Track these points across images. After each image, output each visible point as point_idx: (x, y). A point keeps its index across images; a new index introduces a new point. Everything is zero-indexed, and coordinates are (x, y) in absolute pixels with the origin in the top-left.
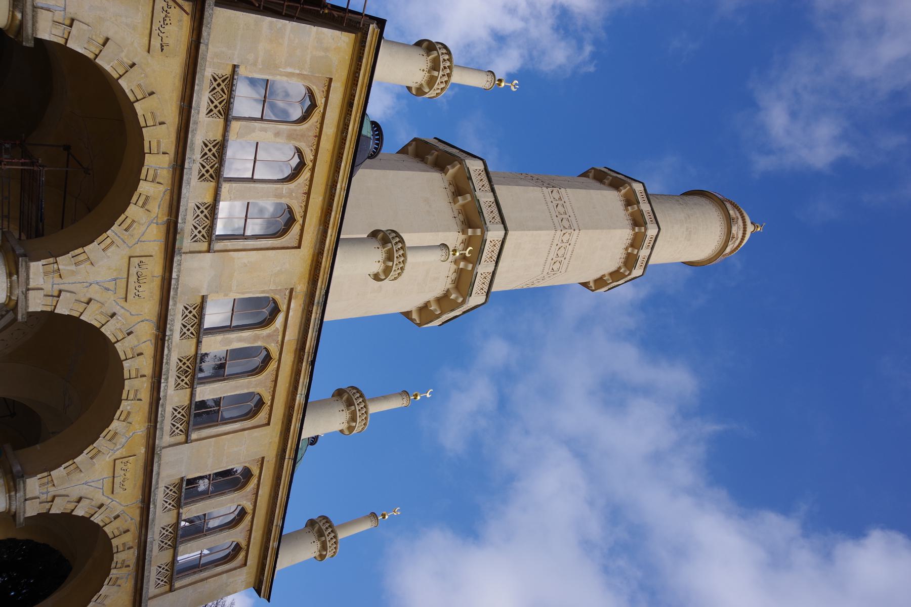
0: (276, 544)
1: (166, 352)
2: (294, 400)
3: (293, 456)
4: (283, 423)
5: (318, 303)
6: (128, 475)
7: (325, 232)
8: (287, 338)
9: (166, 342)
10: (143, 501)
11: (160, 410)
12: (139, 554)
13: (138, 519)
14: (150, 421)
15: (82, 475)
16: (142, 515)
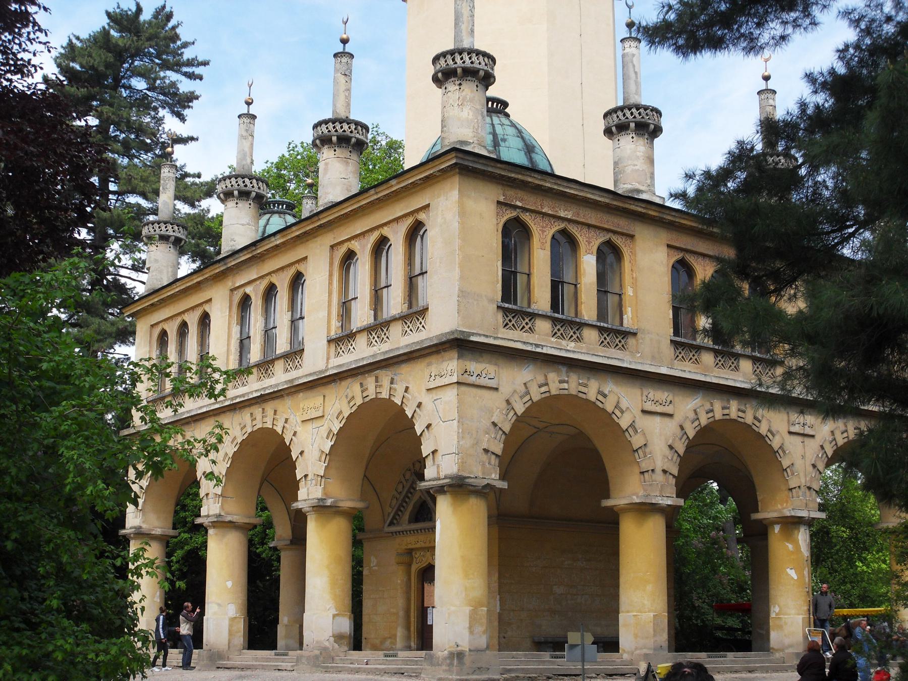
0: (393, 182)
1: (238, 400)
2: (283, 243)
3: (316, 218)
4: (307, 241)
5: (225, 264)
6: (312, 405)
7: (199, 283)
8: (255, 277)
9: (234, 402)
10: (334, 381)
11: (267, 391)
12: (377, 369)
13: (349, 380)
14: (282, 396)
15: (306, 451)
16: (345, 378)
